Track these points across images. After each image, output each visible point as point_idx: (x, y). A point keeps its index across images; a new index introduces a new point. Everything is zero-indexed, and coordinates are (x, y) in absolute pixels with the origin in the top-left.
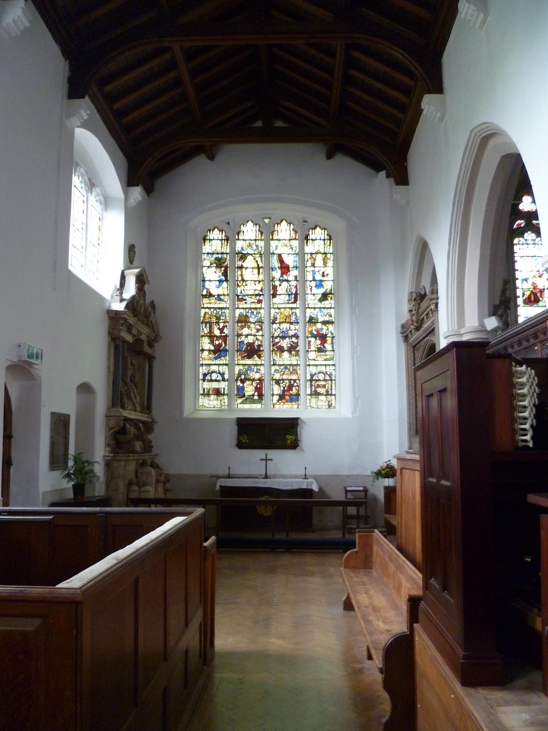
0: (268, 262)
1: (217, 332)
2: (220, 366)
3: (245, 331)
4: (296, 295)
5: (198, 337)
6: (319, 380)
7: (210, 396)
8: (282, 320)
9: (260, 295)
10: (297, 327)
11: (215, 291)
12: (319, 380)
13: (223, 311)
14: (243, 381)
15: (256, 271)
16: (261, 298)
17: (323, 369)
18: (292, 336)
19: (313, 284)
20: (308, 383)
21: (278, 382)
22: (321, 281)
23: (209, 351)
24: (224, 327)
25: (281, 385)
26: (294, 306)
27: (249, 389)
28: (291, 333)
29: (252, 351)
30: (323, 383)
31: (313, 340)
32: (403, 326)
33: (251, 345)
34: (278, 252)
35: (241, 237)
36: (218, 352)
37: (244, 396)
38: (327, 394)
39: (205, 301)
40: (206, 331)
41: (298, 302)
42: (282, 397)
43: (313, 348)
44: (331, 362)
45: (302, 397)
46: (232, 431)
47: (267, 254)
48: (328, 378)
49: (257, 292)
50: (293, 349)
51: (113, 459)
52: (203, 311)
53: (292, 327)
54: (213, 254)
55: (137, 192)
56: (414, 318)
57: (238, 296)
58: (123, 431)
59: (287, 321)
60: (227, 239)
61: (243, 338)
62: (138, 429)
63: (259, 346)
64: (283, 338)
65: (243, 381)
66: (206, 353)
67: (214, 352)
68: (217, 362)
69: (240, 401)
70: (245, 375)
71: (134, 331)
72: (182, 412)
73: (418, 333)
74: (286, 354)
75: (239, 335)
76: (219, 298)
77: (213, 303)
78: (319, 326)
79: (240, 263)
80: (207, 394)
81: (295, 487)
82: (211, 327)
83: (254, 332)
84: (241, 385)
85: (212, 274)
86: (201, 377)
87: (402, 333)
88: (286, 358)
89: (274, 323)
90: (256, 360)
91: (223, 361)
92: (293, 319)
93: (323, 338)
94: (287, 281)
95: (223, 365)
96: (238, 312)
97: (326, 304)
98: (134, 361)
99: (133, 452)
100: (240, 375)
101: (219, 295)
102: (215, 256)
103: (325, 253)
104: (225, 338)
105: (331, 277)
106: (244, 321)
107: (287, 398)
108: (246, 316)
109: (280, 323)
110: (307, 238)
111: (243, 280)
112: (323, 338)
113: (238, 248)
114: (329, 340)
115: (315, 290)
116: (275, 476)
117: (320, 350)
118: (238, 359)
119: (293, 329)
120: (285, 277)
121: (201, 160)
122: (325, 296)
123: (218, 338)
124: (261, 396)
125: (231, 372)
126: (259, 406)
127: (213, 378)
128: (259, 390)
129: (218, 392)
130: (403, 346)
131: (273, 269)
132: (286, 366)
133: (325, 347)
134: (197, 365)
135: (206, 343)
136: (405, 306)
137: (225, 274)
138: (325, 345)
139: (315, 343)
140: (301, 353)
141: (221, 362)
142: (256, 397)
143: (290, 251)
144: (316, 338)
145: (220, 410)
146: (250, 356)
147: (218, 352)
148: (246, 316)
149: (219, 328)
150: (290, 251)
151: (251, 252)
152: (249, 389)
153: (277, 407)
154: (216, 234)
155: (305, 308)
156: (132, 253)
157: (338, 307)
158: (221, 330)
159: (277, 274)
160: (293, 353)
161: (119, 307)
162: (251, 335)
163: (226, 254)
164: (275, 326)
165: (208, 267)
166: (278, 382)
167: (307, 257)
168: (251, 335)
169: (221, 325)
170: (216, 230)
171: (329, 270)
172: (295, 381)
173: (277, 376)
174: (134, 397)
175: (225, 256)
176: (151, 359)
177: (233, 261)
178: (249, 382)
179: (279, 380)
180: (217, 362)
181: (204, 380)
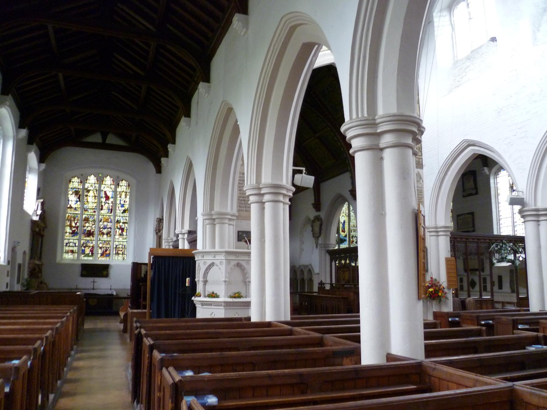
0: (99, 194)
2: (74, 240)
3: (87, 225)
4: (112, 210)
5: (64, 226)
7: (70, 252)
11: (74, 206)
14: (85, 247)
15: (94, 198)
17: (122, 243)
21: (101, 248)
22: (123, 204)
23: (70, 233)
26: (110, 215)
27: (87, 251)
28: (108, 227)
29: (90, 234)
31: (118, 230)
33: (90, 231)
34: (105, 190)
35: (88, 182)
36: (74, 233)
38: (123, 254)
39: (69, 210)
40: (68, 224)
42: (102, 255)
43: (117, 234)
44: (125, 240)
45: (111, 255)
47: (100, 191)
50: (108, 234)
52: (67, 215)
53: (109, 224)
55: (43, 166)
58: (34, 269)
60: (81, 182)
63: (93, 232)
64: (104, 228)
66: (67, 234)
67: (72, 233)
69: (83, 256)
72: (55, 261)
74: (105, 236)
75: (84, 226)
76: (75, 209)
77: (73, 211)
78: (121, 224)
79: (86, 194)
80: (67, 252)
81: (106, 293)
83: (91, 225)
85: (72, 198)
86: (65, 244)
88: (105, 237)
90: (91, 238)
91: (76, 238)
93: (122, 230)
96: (84, 216)
97: (125, 214)
100: (83, 244)
103: (126, 192)
104: (77, 227)
105: (128, 203)
106: (87, 220)
108: (88, 218)
110: (118, 185)
111: (87, 201)
112: (122, 230)
113: (86, 186)
114: (125, 231)
115: (120, 208)
116: (97, 289)
117: (120, 235)
118: (83, 237)
119: (109, 225)
120: (107, 202)
122: (124, 211)
123: (74, 227)
124: (92, 254)
125: (79, 243)
126: (91, 258)
128: (92, 251)
129: (72, 252)
130: (156, 236)
131: (102, 197)
132: (105, 241)
134: (63, 239)
135: (68, 230)
136: (156, 223)
137: (79, 198)
140: (112, 236)
142: (90, 254)
143: (110, 190)
145: (73, 260)
146: (89, 236)
147: (74, 233)
148: (88, 218)
151: (91, 188)
152: (87, 251)
153: (100, 259)
154: (76, 180)
155: (115, 216)
158: (76, 224)
159: (103, 200)
161: (36, 218)
164: (101, 223)
166: (101, 248)
169: (76, 222)
170: (76, 178)
171: (127, 200)
173: (101, 245)
176: (42, 236)
180: (73, 238)
181: (66, 246)
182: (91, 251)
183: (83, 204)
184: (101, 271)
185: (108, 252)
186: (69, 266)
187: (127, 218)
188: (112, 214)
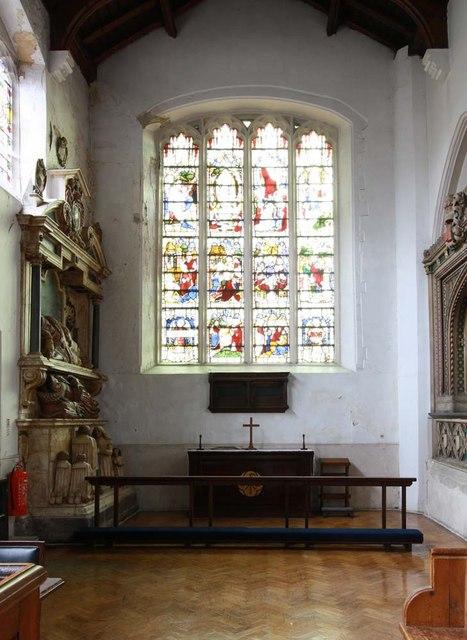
0: (247, 177)
1: (183, 268)
3: (220, 266)
4: (284, 220)
5: (158, 273)
6: (314, 327)
7: (175, 342)
8: (266, 253)
9: (238, 221)
10: (286, 260)
12: (314, 327)
13: (191, 240)
14: (217, 329)
16: (241, 224)
17: (317, 313)
18: (279, 273)
19: (306, 205)
20: (300, 330)
21: (261, 329)
24: (192, 261)
25: (266, 333)
27: (225, 338)
29: (228, 292)
30: (320, 330)
32: (427, 253)
33: (228, 283)
35: (214, 145)
36: (184, 291)
37: (218, 347)
41: (287, 230)
42: (266, 348)
46: (203, 393)
47: (247, 168)
48: (324, 324)
49: (234, 217)
51: (31, 426)
52: (165, 241)
53: (280, 261)
54: (178, 167)
56: (455, 230)
57: (210, 222)
59: (275, 253)
60: (196, 149)
61: (217, 275)
62: (73, 385)
63: (238, 285)
65: (217, 329)
67: (180, 292)
68: (185, 305)
69: (213, 353)
70: (219, 321)
71: (64, 253)
73: (456, 255)
78: (314, 259)
79: (211, 180)
82: (175, 262)
84: (215, 334)
86: (164, 324)
87: (424, 262)
88: (272, 300)
89: (256, 256)
92: (281, 250)
94: (273, 202)
95: (192, 308)
98: (71, 299)
99: (63, 415)
101: (185, 221)
102: (181, 170)
103: (322, 167)
107: (273, 349)
109: (264, 256)
111: (217, 202)
112: (319, 274)
114: (326, 277)
118: (211, 299)
119: (283, 264)
120: (270, 198)
121: (158, 39)
125: (202, 319)
127: (180, 325)
128: (237, 339)
129: (186, 343)
130: (426, 279)
133: (321, 286)
137: (194, 194)
138: (322, 283)
139: (308, 281)
141: (190, 305)
142: (234, 349)
144: (309, 274)
149: (186, 263)
150: (278, 164)
154: (181, 142)
155: (295, 237)
156: (62, 151)
157: (337, 236)
158: (189, 265)
159: (259, 193)
160: (281, 293)
162: (227, 271)
163: (195, 167)
165: (172, 184)
166: (261, 329)
167: (299, 171)
168: (227, 271)
169: (189, 259)
172: (283, 328)
173: (260, 323)
174: (67, 344)
175: (193, 170)
176: (95, 298)
177: (203, 175)
178: (227, 330)
179: (263, 327)
181: (168, 328)
182: (234, 337)
183: (204, 208)
184: (267, 392)
185: (282, 340)
186: (169, 384)
187: (331, 242)
188: (286, 232)
